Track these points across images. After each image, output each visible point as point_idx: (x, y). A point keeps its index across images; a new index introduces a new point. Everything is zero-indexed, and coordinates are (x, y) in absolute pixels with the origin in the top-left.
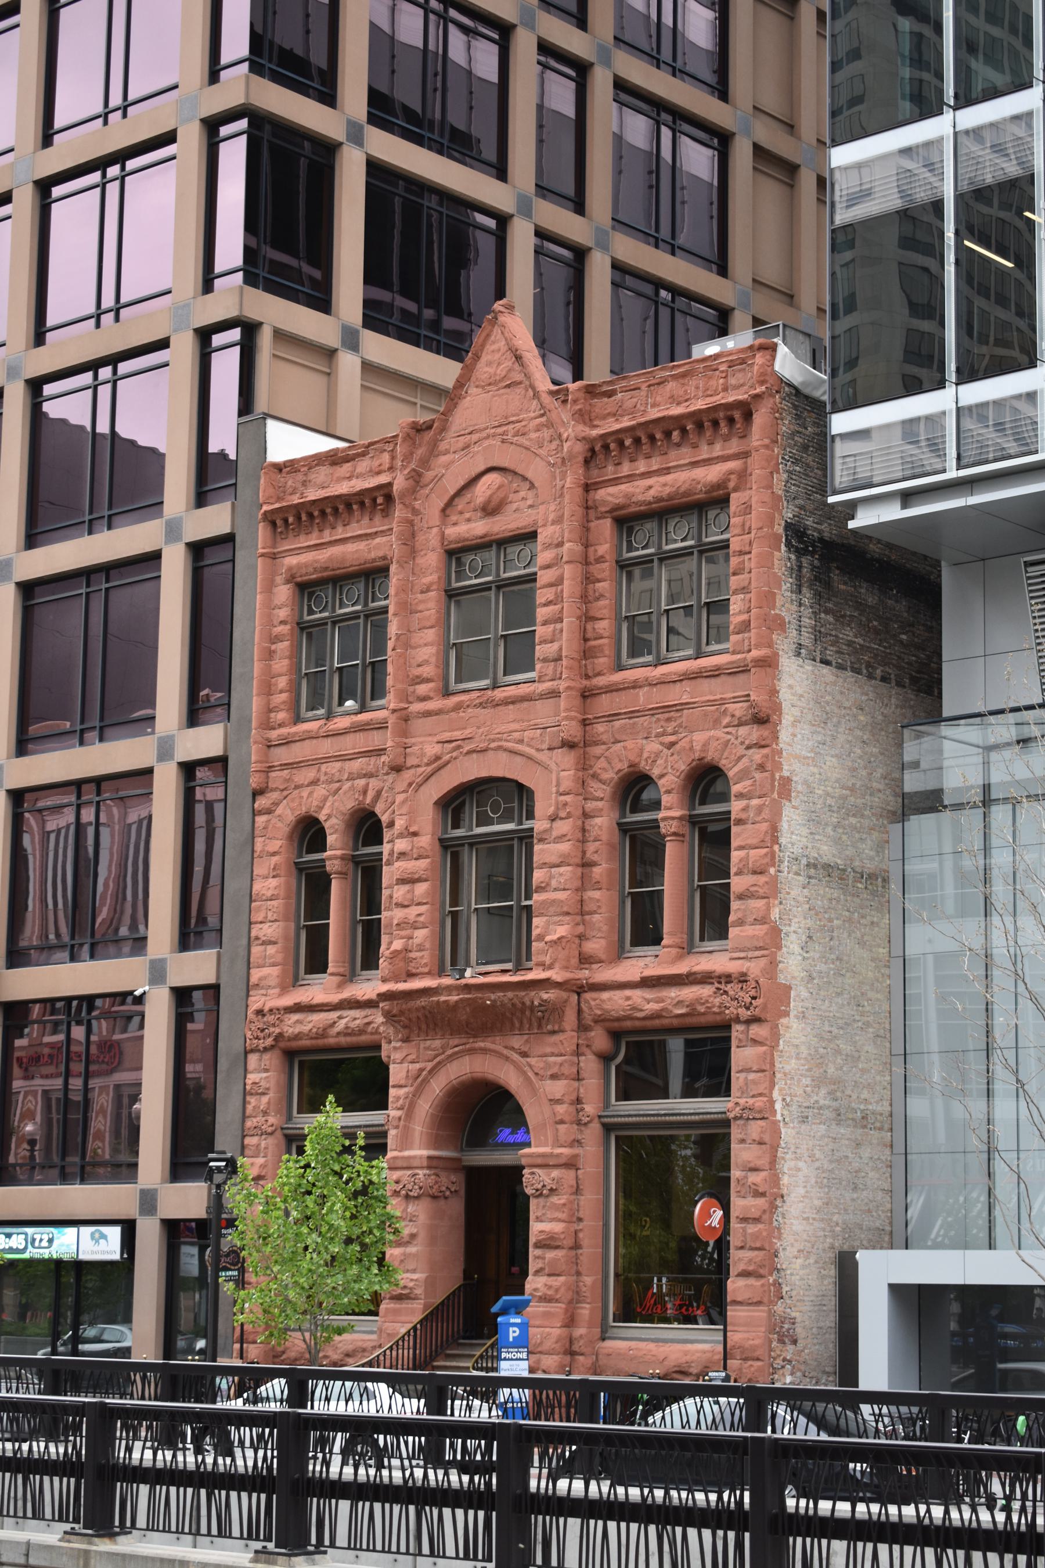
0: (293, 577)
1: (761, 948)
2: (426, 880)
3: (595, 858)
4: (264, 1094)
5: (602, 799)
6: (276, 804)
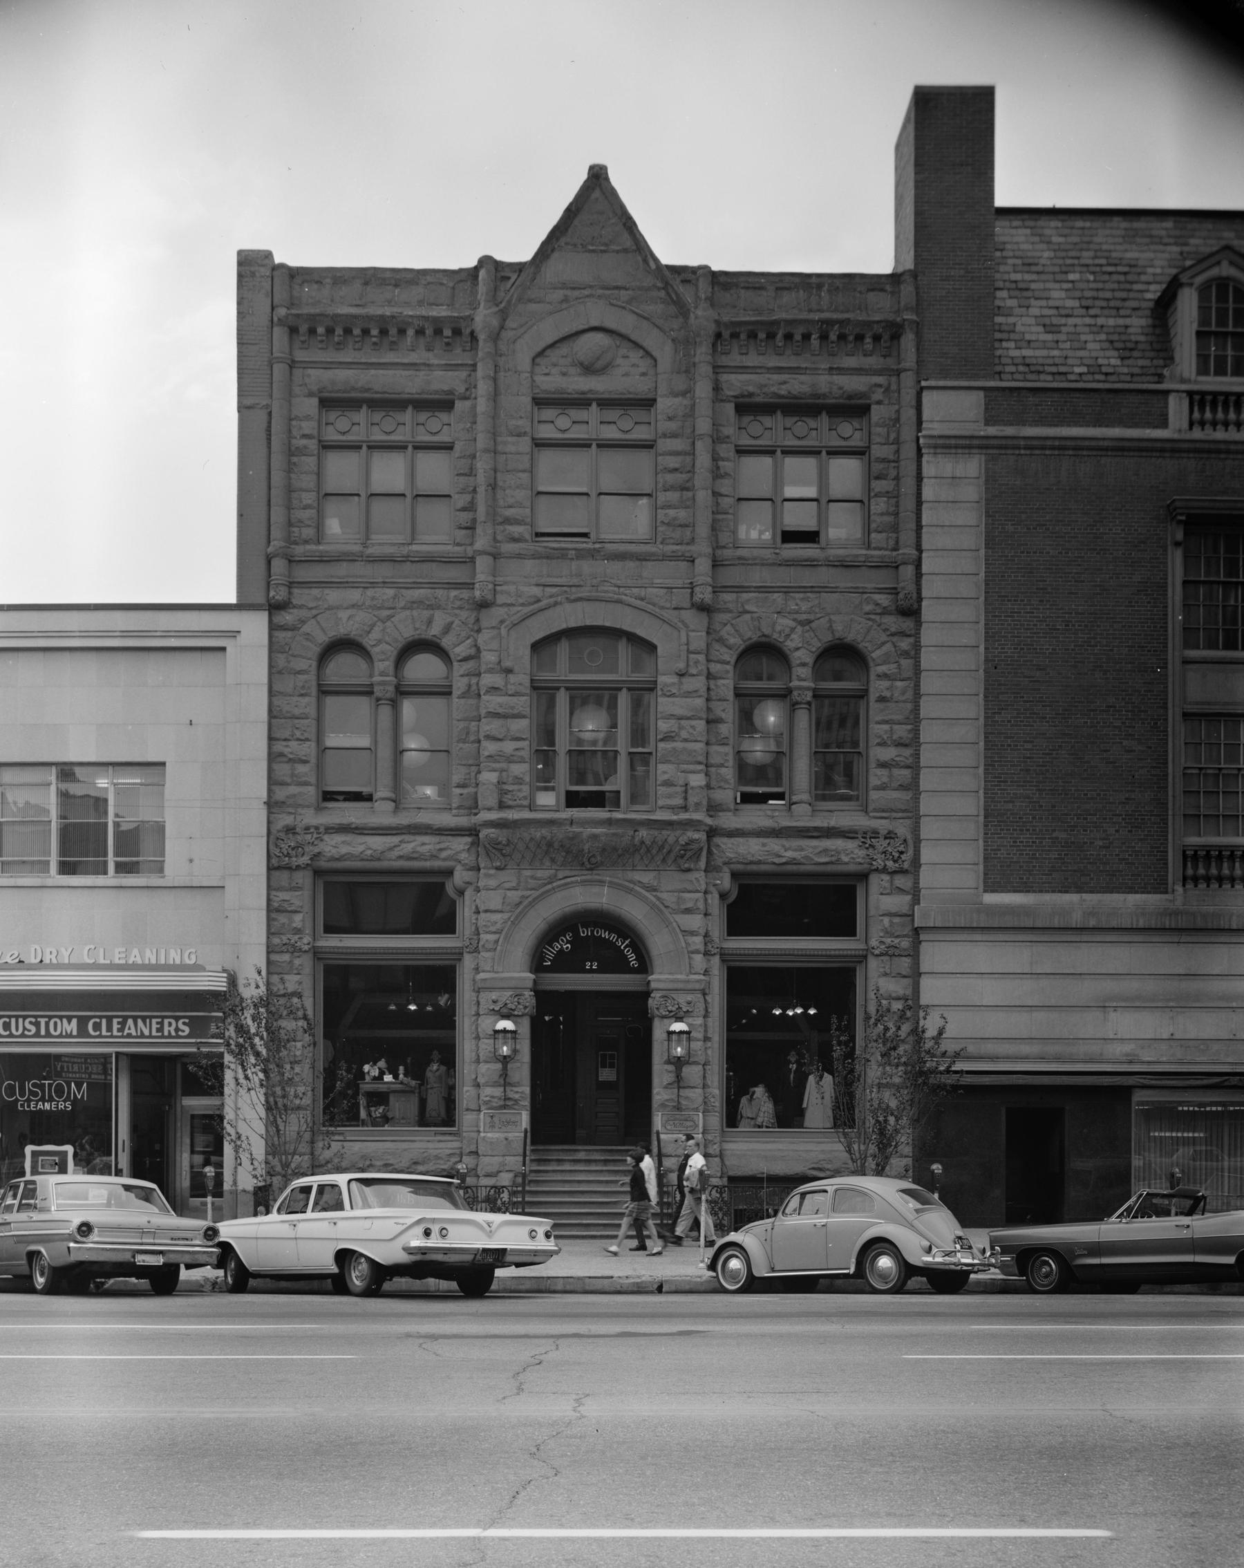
0: (320, 391)
1: (904, 811)
2: (524, 717)
3: (723, 715)
4: (296, 912)
5: (728, 663)
6: (303, 622)
